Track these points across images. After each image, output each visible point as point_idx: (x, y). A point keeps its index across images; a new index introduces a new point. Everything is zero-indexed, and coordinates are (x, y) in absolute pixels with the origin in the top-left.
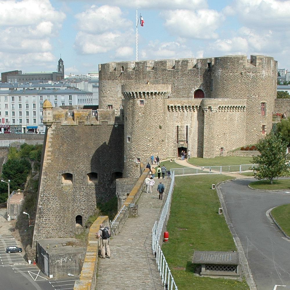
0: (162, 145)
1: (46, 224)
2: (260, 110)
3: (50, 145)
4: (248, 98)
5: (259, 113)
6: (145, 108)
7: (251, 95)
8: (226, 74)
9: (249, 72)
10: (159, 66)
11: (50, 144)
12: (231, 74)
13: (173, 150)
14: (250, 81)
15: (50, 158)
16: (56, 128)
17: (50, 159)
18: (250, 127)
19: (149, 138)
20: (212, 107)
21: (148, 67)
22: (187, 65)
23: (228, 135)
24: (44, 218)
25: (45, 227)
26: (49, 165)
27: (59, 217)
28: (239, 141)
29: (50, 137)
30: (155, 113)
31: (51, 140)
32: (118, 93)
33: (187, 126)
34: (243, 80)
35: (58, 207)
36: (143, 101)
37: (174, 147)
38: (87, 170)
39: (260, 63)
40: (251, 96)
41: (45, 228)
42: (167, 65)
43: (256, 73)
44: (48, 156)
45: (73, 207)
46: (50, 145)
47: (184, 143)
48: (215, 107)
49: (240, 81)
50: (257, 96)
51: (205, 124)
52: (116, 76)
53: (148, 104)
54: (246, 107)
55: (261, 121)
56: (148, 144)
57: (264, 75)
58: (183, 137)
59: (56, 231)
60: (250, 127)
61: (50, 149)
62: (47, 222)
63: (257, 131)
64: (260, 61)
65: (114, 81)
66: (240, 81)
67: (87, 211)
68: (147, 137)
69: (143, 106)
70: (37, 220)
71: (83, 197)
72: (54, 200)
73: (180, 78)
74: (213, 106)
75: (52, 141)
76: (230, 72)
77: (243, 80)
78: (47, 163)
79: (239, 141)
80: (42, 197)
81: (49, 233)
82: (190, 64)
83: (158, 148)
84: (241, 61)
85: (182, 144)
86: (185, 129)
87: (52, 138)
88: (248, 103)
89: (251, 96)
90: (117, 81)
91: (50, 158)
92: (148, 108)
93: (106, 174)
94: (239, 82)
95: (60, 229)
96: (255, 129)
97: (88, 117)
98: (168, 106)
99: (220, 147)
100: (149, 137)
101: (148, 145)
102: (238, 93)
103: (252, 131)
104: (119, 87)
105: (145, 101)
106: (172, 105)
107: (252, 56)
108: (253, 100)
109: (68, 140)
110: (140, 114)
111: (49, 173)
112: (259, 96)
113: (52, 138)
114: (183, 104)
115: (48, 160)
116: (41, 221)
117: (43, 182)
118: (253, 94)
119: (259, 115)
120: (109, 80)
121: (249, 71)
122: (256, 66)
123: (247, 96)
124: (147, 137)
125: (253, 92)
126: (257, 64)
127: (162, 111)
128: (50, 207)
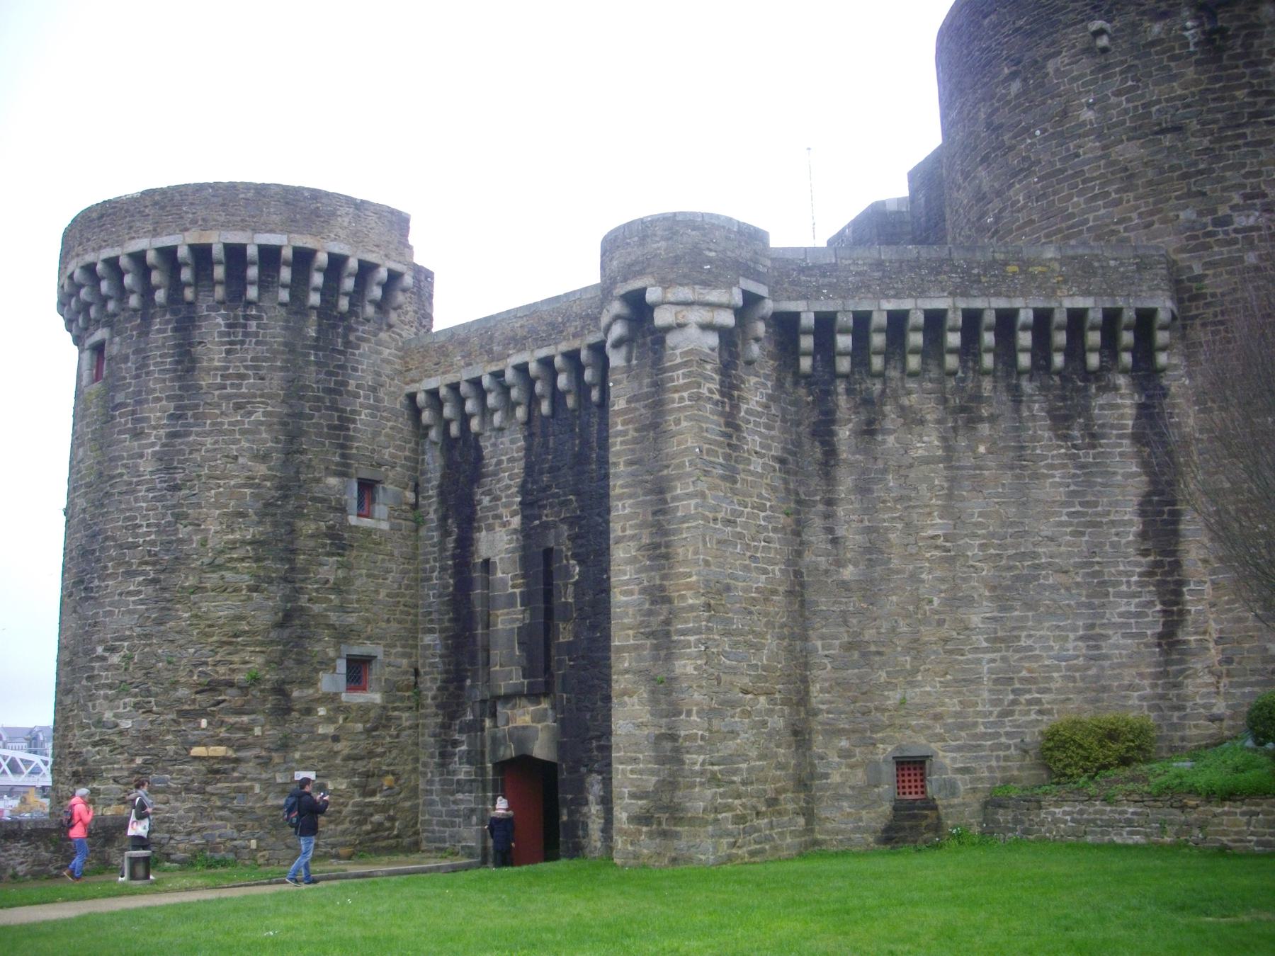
7: (1223, 210)
19: (115, 659)
20: (652, 295)
28: (1131, 687)
34: (1118, 94)
40: (1224, 221)
48: (684, 293)
49: (1088, 115)
74: (665, 283)
77: (1113, 100)
79: (1131, 687)
83: (197, 751)
94: (1083, 124)
99: (885, 751)
100: (112, 650)
102: (1091, 216)
106: (431, 383)
118: (1236, 199)
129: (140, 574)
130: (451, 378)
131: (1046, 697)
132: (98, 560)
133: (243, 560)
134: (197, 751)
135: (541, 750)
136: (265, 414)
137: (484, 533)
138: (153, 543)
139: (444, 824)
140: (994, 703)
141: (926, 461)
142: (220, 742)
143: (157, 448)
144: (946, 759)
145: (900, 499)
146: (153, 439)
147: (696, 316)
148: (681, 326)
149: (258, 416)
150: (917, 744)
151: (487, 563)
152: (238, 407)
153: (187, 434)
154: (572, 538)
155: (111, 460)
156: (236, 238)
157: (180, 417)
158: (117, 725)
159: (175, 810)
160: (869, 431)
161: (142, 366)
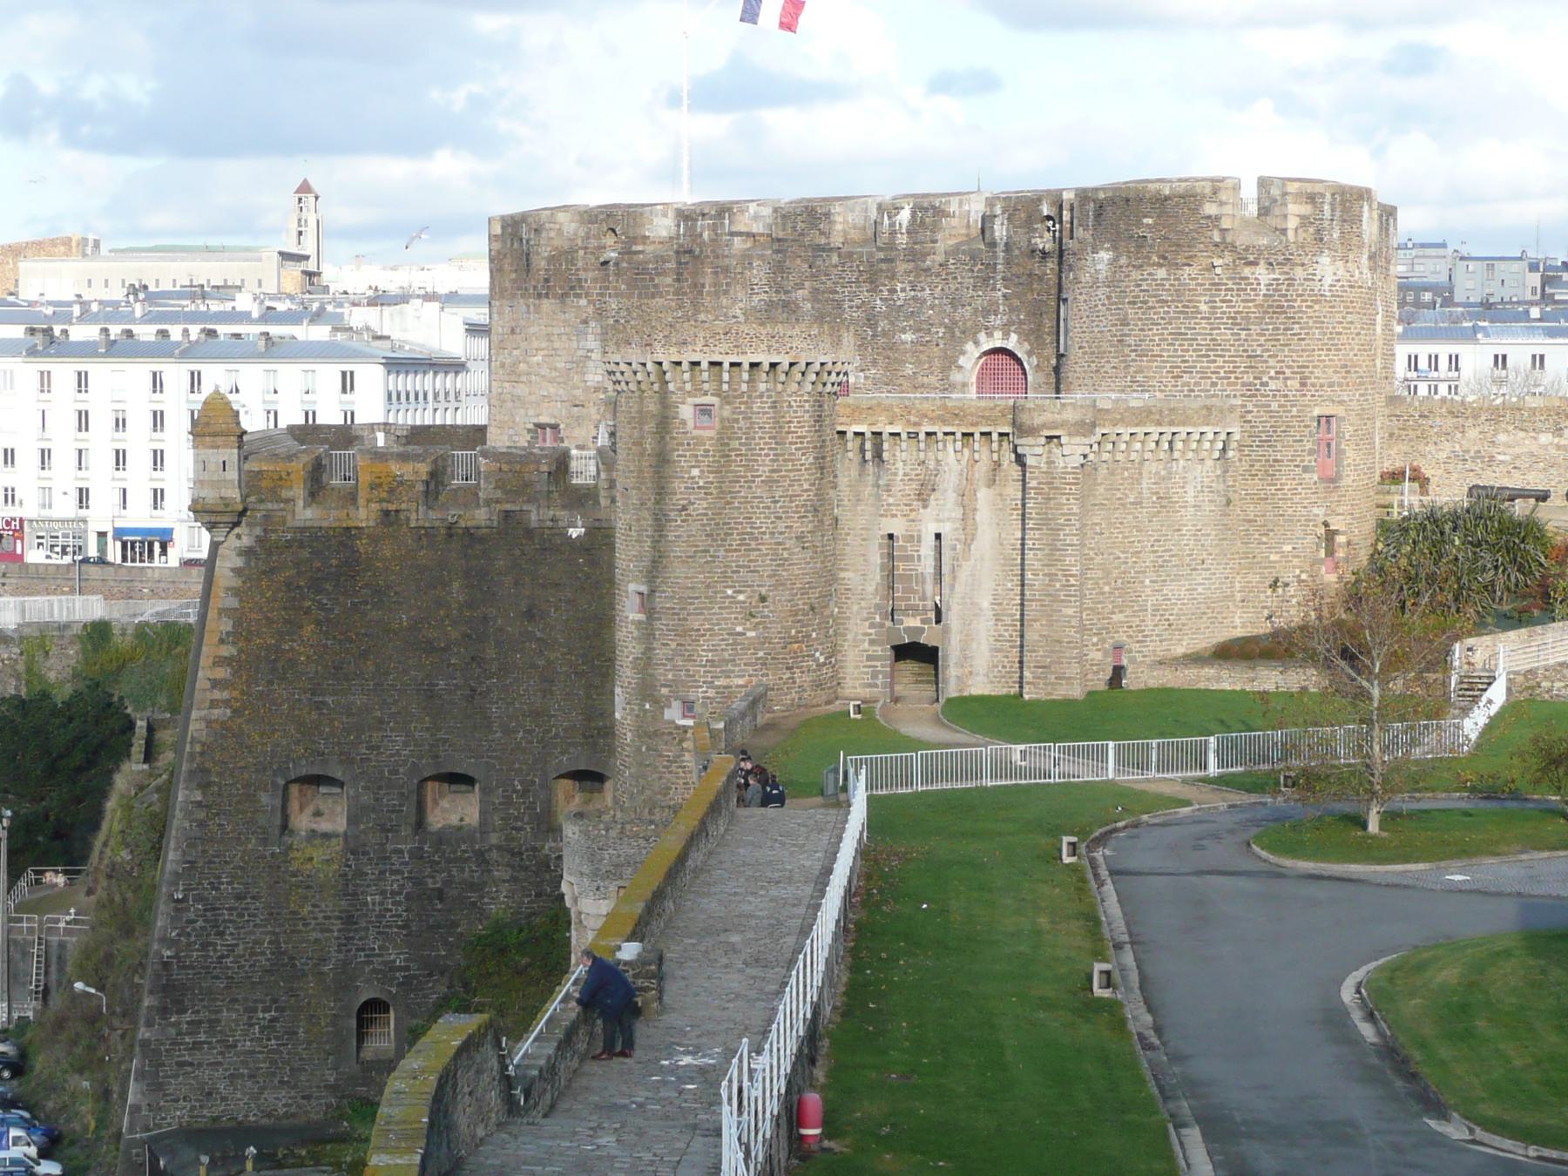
1: (197, 1046)
2: (1311, 452)
3: (229, 628)
4: (1251, 391)
5: (1306, 469)
6: (723, 441)
8: (1135, 275)
10: (794, 228)
11: (227, 625)
12: (1162, 273)
13: (869, 658)
15: (225, 695)
16: (259, 540)
17: (226, 703)
18: (1264, 539)
19: (741, 597)
21: (740, 234)
22: (935, 227)
23: (1147, 582)
24: (188, 1017)
25: (191, 1064)
26: (221, 730)
27: (266, 1010)
29: (228, 589)
30: (773, 471)
31: (233, 602)
32: (591, 364)
33: (938, 536)
34: (1223, 301)
35: (263, 953)
37: (872, 642)
38: (420, 757)
39: (1302, 217)
41: (189, 1069)
42: (839, 227)
43: (1286, 269)
44: (215, 684)
45: (341, 956)
46: (229, 628)
47: (923, 621)
49: (1204, 308)
50: (1294, 384)
52: (580, 280)
53: (737, 421)
54: (1237, 437)
56: (739, 629)
57: (1328, 281)
58: (915, 592)
59: (249, 1083)
60: (1264, 539)
61: (228, 651)
62: (202, 1037)
63: (1296, 561)
64: (1306, 209)
65: (568, 301)
66: (1204, 308)
67: (414, 977)
68: (730, 592)
69: (712, 433)
70: (149, 1024)
71: (398, 903)
72: (241, 915)
73: (903, 290)
75: (236, 605)
78: (209, 723)
80: (178, 901)
81: (210, 1094)
82: (955, 222)
84: (1210, 209)
86: (927, 548)
87: (236, 592)
88: (1249, 417)
89: (1262, 384)
90: (583, 302)
91: (225, 695)
93: (521, 782)
95: (274, 1074)
97: (432, 486)
100: (740, 592)
101: (739, 634)
103: (1273, 557)
104: (590, 337)
105: (721, 408)
107: (1264, 183)
108: (1274, 406)
109: (322, 607)
110: (695, 472)
111: (220, 774)
112: (1303, 384)
113: (236, 592)
114: (915, 424)
115: (214, 704)
116: (173, 1031)
117: (187, 825)
118: (1272, 373)
119: (1306, 476)
120: (539, 296)
121: (1251, 258)
122: (1284, 231)
123: (1244, 384)
124: (730, 592)
125: (1272, 362)
126: (1292, 223)
128: (223, 957)
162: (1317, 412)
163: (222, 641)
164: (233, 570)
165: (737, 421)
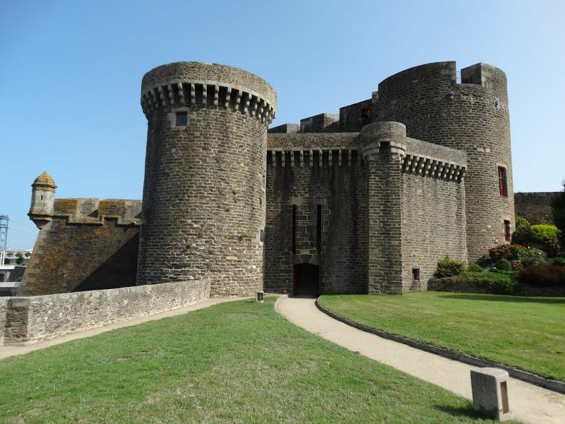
0: (239, 251)
3: (38, 262)
7: (475, 146)
9: (466, 95)
14: (470, 114)
19: (195, 226)
20: (392, 144)
36: (185, 113)
40: (475, 149)
47: (311, 252)
48: (399, 145)
51: (372, 193)
55: (500, 210)
64: (489, 74)
68: (190, 221)
76: (420, 97)
83: (228, 258)
84: (443, 72)
85: (305, 253)
92: (198, 134)
96: (489, 226)
98: (269, 153)
100: (196, 222)
103: (483, 230)
108: (480, 159)
121: (466, 93)
124: (190, 221)
126: (483, 79)
127: (246, 151)
129: (208, 197)
130: (286, 149)
131: (439, 256)
132: (188, 190)
133: (241, 197)
134: (228, 258)
135: (312, 261)
136: (248, 151)
137: (293, 197)
138: (214, 188)
139: (274, 282)
140: (431, 257)
141: (420, 196)
142: (235, 255)
143: (214, 155)
144: (421, 270)
145: (415, 204)
146: (212, 151)
147: (400, 152)
148: (397, 154)
149: (246, 151)
150: (416, 265)
151: (295, 207)
152: (241, 146)
153: (226, 152)
154: (328, 203)
155: (193, 156)
156: (246, 90)
157: (223, 146)
158: (197, 248)
159: (220, 277)
160: (409, 186)
161: (208, 125)
162: (498, 164)
163: (34, 267)
164: (44, 240)
165: (199, 121)
